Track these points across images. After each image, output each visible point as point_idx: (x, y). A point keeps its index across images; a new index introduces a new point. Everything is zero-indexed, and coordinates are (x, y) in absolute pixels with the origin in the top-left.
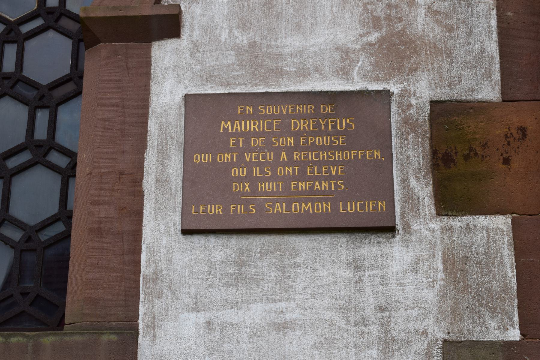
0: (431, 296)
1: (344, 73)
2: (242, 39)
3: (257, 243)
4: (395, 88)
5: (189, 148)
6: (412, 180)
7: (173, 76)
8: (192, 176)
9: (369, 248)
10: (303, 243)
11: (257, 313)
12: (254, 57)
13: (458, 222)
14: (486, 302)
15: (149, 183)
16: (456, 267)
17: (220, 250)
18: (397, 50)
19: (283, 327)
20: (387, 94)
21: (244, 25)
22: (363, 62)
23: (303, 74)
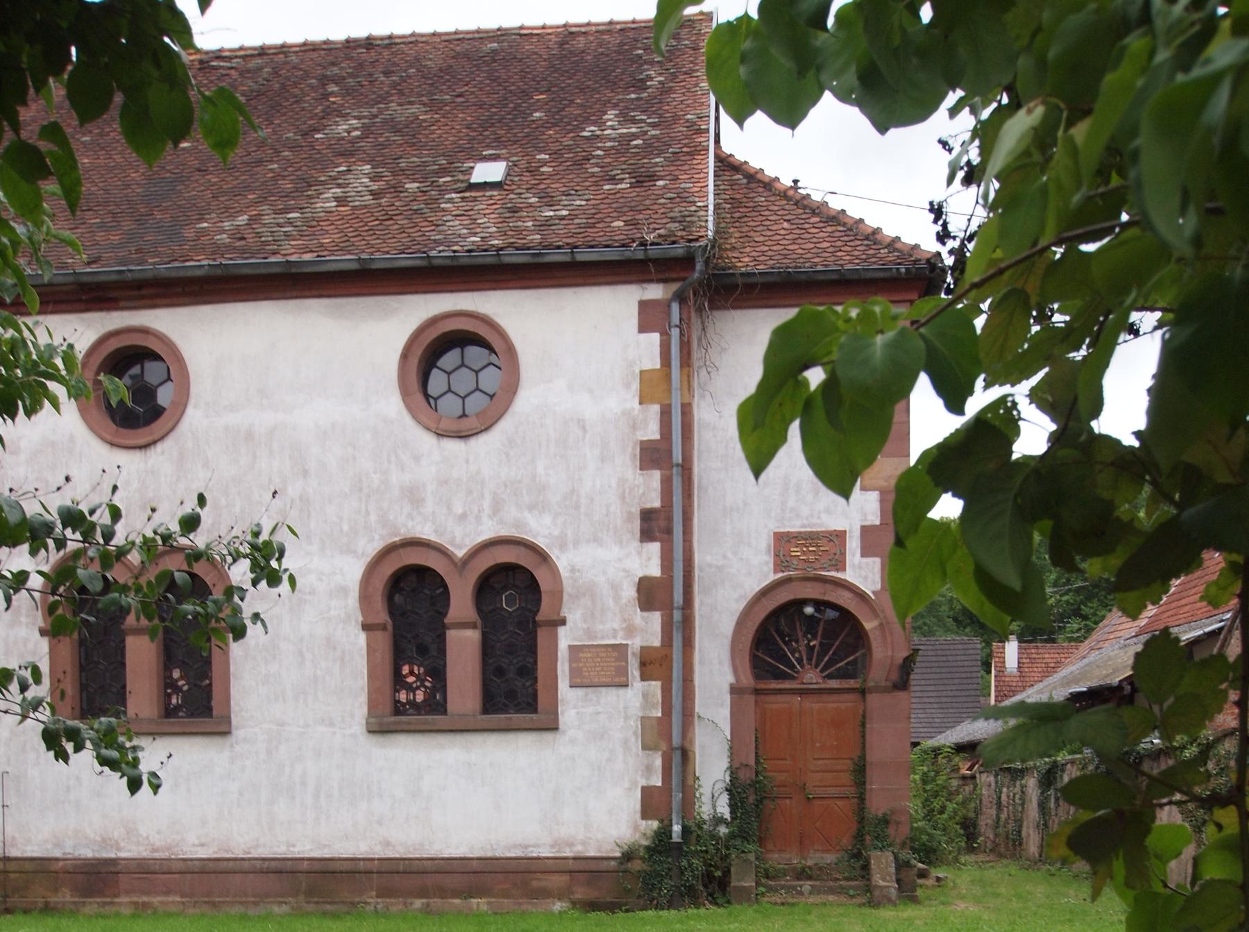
0: (638, 704)
1: (615, 637)
2: (585, 626)
3: (590, 690)
4: (629, 642)
5: (571, 661)
6: (634, 671)
7: (565, 639)
8: (571, 670)
9: (621, 691)
10: (603, 690)
11: (591, 709)
12: (589, 633)
13: (646, 683)
14: (654, 706)
15: (559, 673)
16: (645, 696)
17: (580, 692)
18: (630, 630)
19: (598, 713)
20: (627, 645)
21: (585, 621)
22: (621, 634)
23: (603, 638)
